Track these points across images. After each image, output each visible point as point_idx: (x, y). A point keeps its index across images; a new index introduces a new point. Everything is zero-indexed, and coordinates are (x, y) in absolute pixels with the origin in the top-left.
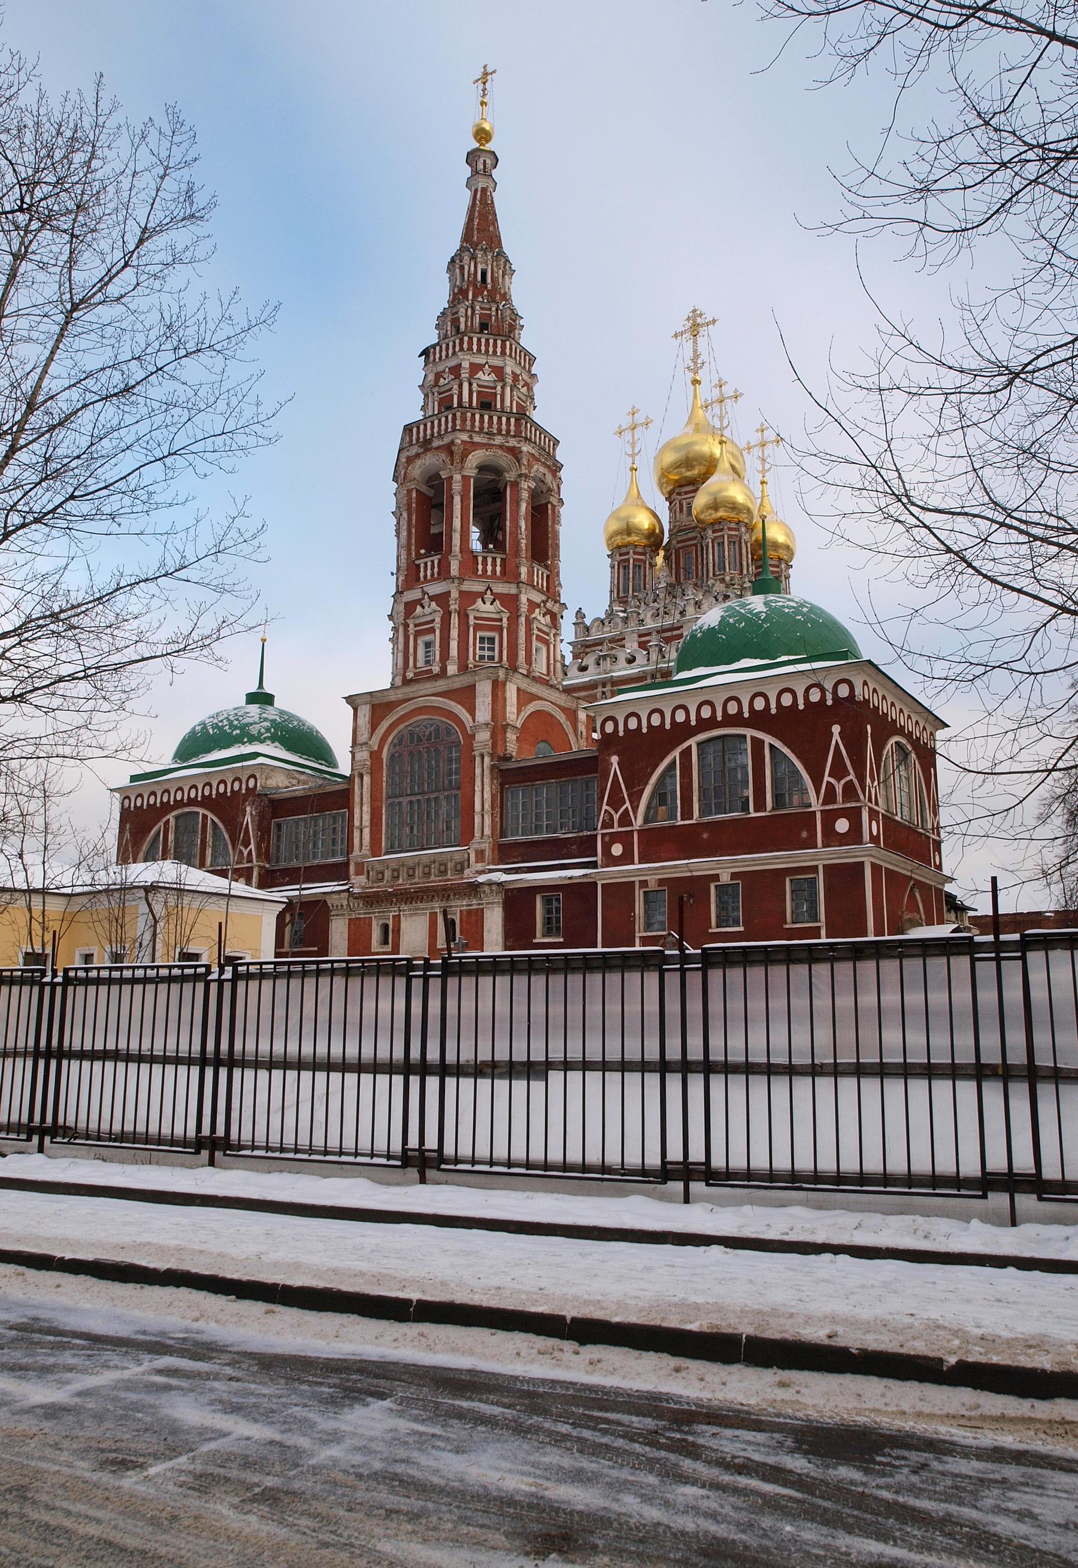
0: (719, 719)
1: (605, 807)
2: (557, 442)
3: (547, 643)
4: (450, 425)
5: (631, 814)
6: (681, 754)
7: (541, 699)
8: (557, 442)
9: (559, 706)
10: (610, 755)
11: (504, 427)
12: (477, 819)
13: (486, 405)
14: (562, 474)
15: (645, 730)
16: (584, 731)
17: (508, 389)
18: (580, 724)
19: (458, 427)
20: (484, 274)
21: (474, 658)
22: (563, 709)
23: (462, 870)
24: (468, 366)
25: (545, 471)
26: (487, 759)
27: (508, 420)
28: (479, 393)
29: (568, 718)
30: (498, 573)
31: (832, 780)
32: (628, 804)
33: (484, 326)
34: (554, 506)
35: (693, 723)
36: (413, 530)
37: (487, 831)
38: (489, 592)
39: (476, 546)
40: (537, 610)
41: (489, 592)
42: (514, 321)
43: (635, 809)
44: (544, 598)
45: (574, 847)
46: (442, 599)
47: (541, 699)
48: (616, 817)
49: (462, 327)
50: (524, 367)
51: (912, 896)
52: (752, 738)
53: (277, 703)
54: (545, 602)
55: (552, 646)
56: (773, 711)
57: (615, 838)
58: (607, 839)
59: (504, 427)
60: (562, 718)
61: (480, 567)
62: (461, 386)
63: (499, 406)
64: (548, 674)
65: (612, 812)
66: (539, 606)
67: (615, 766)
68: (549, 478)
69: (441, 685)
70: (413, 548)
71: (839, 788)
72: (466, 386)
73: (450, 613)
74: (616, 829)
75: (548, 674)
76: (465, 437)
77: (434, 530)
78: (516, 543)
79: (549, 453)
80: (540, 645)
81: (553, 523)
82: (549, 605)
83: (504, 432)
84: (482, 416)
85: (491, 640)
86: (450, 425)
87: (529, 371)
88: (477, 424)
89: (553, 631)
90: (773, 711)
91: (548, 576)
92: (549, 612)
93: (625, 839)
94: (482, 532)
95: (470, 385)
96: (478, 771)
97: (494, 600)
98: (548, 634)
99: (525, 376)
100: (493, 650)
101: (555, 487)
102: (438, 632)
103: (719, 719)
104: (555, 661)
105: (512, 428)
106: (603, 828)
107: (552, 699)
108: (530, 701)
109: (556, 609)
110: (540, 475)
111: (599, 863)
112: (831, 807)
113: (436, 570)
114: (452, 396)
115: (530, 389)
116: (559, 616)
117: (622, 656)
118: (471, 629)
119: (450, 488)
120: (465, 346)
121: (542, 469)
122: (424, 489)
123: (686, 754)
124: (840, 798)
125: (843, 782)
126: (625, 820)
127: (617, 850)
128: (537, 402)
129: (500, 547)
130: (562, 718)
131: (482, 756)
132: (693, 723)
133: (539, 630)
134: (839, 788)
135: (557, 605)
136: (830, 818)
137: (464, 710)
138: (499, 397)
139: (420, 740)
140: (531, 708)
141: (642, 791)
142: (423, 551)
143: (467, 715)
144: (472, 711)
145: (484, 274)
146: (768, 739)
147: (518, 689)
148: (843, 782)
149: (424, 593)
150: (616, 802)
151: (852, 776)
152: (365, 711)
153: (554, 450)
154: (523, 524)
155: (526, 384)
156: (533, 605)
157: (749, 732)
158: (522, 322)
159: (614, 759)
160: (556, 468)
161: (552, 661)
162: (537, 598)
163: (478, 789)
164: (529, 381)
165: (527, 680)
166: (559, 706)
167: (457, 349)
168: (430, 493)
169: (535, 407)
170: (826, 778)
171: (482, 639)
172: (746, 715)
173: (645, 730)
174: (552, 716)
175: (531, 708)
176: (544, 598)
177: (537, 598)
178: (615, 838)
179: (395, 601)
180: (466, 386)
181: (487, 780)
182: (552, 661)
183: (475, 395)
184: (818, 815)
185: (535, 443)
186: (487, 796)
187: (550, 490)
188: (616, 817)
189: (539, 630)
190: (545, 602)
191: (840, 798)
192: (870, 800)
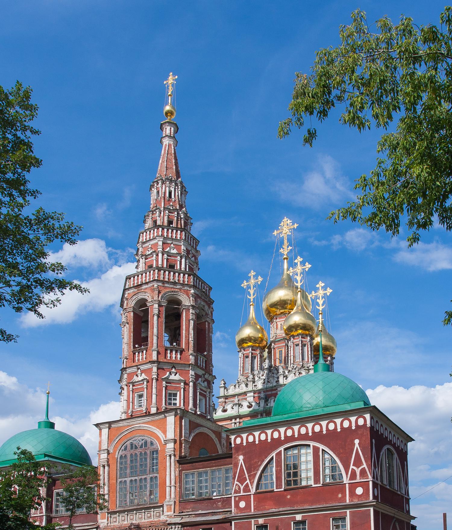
0: (296, 436)
1: (236, 482)
2: (210, 288)
3: (205, 396)
4: (152, 277)
5: (250, 485)
6: (277, 454)
7: (202, 426)
8: (210, 288)
9: (212, 430)
10: (238, 455)
11: (181, 279)
12: (168, 489)
13: (171, 267)
14: (214, 306)
15: (257, 442)
16: (225, 443)
17: (183, 260)
18: (222, 440)
19: (156, 278)
20: (170, 193)
21: (166, 404)
22: (214, 432)
23: (159, 516)
24: (161, 244)
25: (205, 304)
26: (173, 457)
27: (184, 275)
28: (167, 259)
29: (217, 436)
30: (179, 359)
31: (354, 468)
32: (248, 481)
33: (170, 222)
34: (209, 323)
35: (283, 438)
36: (132, 334)
37: (173, 496)
38: (173, 369)
39: (168, 344)
40: (200, 379)
41: (173, 369)
42: (187, 220)
43: (252, 483)
44: (204, 372)
45: (220, 503)
46: (148, 372)
47: (202, 426)
48: (242, 488)
49: (159, 223)
50: (193, 247)
51: (394, 525)
52: (314, 447)
53: (56, 428)
54: (204, 375)
55: (208, 398)
56: (324, 432)
57: (241, 498)
58: (237, 499)
59: (181, 279)
60: (213, 436)
61: (169, 355)
62: (157, 255)
63: (178, 267)
64: (206, 413)
65: (240, 485)
66: (200, 377)
67: (241, 461)
68: (206, 307)
69: (147, 419)
70: (132, 344)
71: (358, 471)
72: (160, 255)
73: (153, 379)
74: (242, 493)
75: (206, 413)
76: (160, 284)
77: (143, 335)
78: (188, 343)
79: (206, 294)
80: (202, 397)
81: (209, 332)
82: (206, 376)
83: (182, 282)
84: (169, 273)
85: (175, 395)
86: (152, 277)
87: (196, 249)
88: (167, 277)
89: (209, 390)
90: (324, 432)
91: (206, 361)
92: (206, 380)
93: (247, 499)
94: (170, 336)
95: (163, 255)
96: (168, 464)
97: (176, 373)
98: (205, 392)
99: (193, 251)
100: (176, 399)
101: (210, 313)
102: (145, 389)
103: (296, 436)
104: (209, 406)
105: (186, 280)
106: (235, 493)
107: (208, 426)
108: (196, 428)
109: (210, 378)
110: (201, 306)
111: (233, 511)
112: (354, 481)
113: (144, 356)
114: (153, 260)
115: (196, 259)
116: (211, 382)
117: (245, 404)
118: (164, 388)
119: (152, 311)
120: (160, 233)
121: (203, 303)
122: (137, 312)
123: (279, 454)
124: (358, 477)
125: (360, 468)
126: (247, 489)
127: (242, 504)
128: (200, 266)
129: (179, 344)
130: (213, 436)
131: (170, 456)
132: (283, 438)
133: (201, 389)
134: (358, 471)
135: (211, 376)
136: (353, 487)
137: (160, 432)
138: (178, 262)
139: (136, 447)
140: (197, 431)
141: (255, 474)
142: (137, 346)
143: (162, 434)
144: (165, 432)
145: (170, 193)
146: (321, 447)
147: (190, 421)
148: (360, 468)
149: (138, 369)
150: (242, 480)
151: (365, 466)
152: (105, 431)
153: (209, 292)
154: (192, 332)
155: (194, 256)
156: (197, 376)
157: (312, 443)
158: (192, 221)
159: (241, 458)
160: (210, 303)
161: (208, 406)
162: (201, 372)
163: (168, 473)
164: (195, 254)
165: (195, 416)
166: (212, 430)
167: (156, 235)
168: (142, 314)
169: (199, 269)
170: (352, 467)
171: (170, 394)
172: (310, 434)
173: (257, 442)
174: (208, 435)
175: (197, 431)
176: (204, 372)
177: (201, 372)
178: (241, 498)
179: (122, 373)
180: (160, 255)
181: (173, 469)
182: (208, 406)
183: (165, 260)
184: (347, 485)
185: (199, 288)
186: (173, 477)
187: (207, 314)
188: (242, 488)
189: (201, 389)
190: (204, 375)
191: (358, 477)
192: (373, 478)
